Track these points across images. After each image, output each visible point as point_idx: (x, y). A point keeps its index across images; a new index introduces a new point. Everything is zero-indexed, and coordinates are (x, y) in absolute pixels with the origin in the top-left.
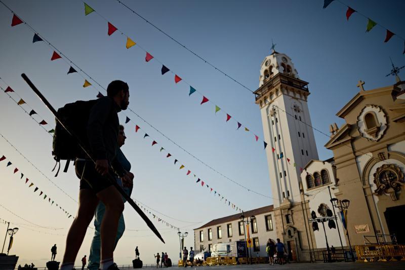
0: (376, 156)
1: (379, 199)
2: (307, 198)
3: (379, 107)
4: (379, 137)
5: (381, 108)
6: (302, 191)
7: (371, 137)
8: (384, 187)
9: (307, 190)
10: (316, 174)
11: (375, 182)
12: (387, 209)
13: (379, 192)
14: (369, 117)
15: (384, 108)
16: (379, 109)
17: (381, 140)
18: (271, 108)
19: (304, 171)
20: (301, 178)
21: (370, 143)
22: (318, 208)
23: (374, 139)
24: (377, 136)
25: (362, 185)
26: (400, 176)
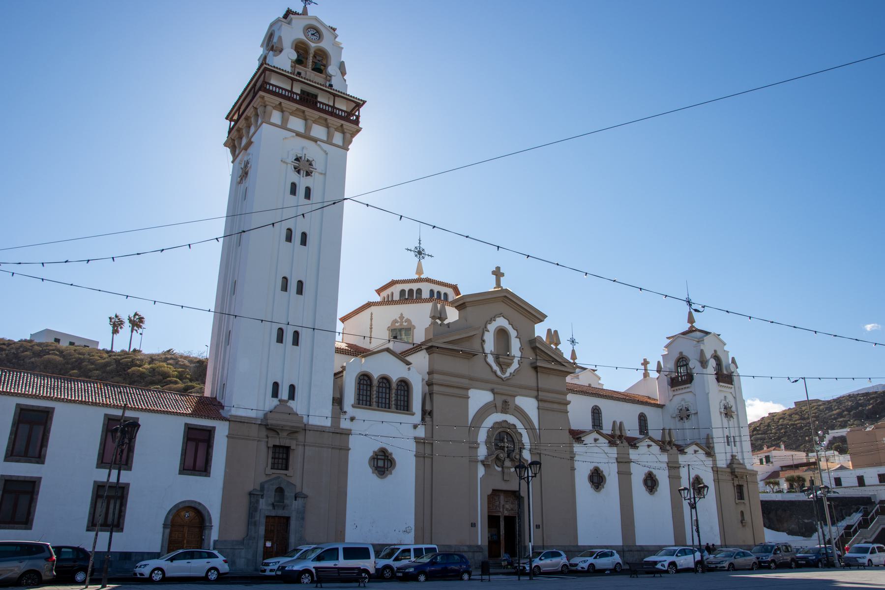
0: (499, 405)
2: (345, 424)
4: (507, 374)
6: (338, 401)
7: (496, 367)
9: (353, 406)
10: (385, 380)
12: (494, 490)
22: (371, 454)
24: (503, 371)
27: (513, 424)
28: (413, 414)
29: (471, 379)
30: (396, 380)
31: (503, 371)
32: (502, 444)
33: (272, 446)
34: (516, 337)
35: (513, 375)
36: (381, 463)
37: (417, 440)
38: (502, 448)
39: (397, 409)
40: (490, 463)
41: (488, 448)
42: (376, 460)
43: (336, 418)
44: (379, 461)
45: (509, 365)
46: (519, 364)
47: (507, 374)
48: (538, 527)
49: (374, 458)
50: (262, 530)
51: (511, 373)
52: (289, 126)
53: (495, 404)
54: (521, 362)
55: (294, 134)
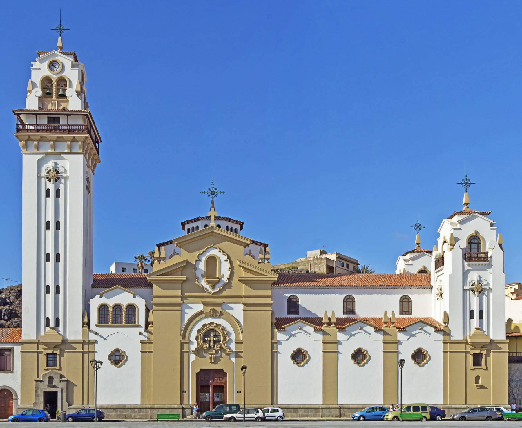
3: (227, 254)
5: (229, 257)
8: (207, 347)
9: (97, 326)
10: (117, 307)
11: (197, 338)
12: (201, 370)
13: (197, 352)
14: (212, 261)
15: (232, 260)
16: (226, 257)
18: (50, 165)
19: (98, 297)
20: (89, 305)
23: (210, 290)
25: (180, 338)
26: (225, 339)
30: (126, 306)
33: (46, 354)
36: (118, 358)
37: (142, 342)
39: (126, 324)
42: (114, 356)
43: (86, 334)
49: (113, 355)
50: (42, 399)
52: (41, 151)
55: (44, 155)
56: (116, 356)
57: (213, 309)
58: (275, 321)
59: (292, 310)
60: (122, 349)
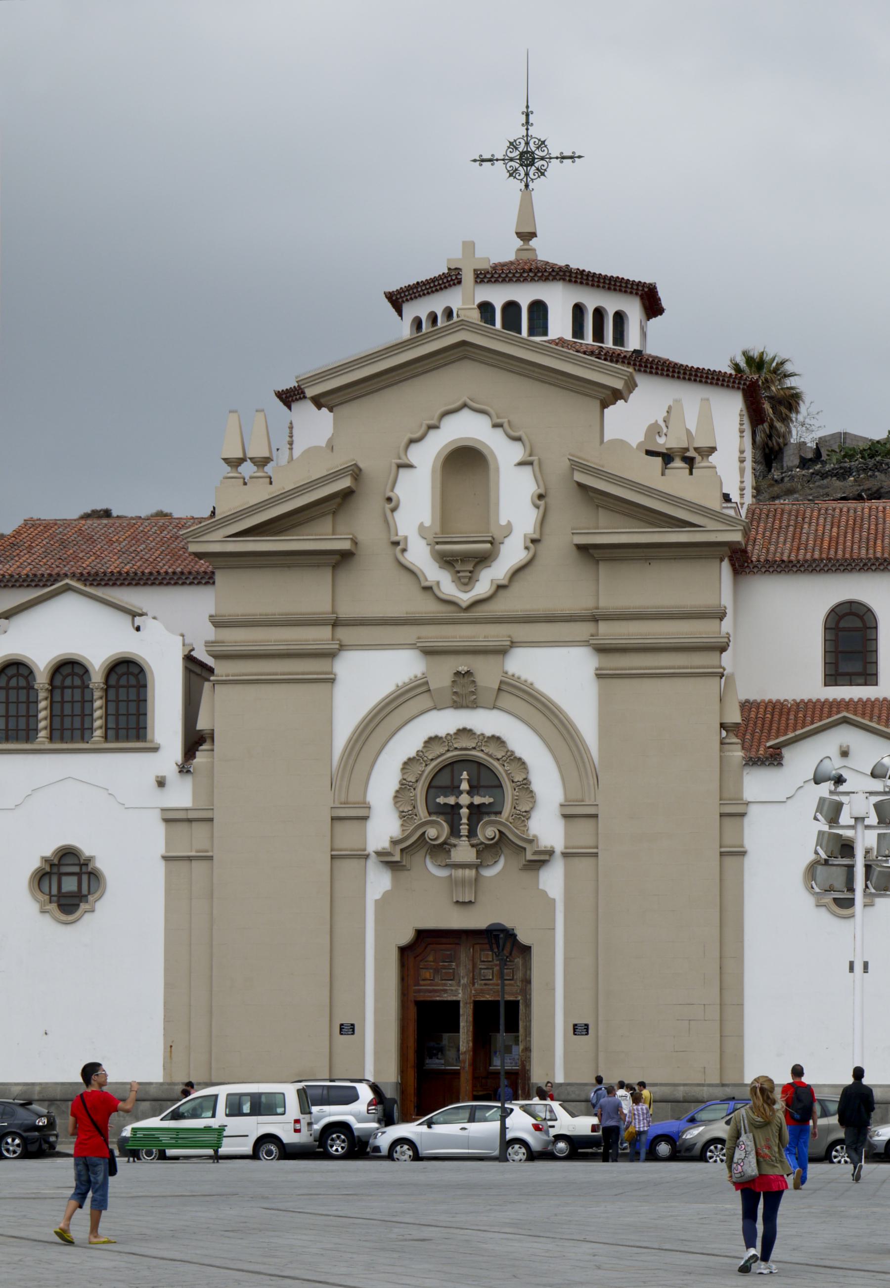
1: (395, 881)
4: (482, 587)
17: (477, 613)
21: (427, 607)
22: (35, 864)
24: (467, 581)
27: (493, 736)
28: (155, 749)
29: (336, 623)
31: (467, 581)
32: (451, 800)
34: (521, 464)
35: (500, 587)
36: (70, 885)
38: (451, 813)
40: (397, 858)
41: (405, 817)
44: (65, 879)
45: (483, 559)
46: (527, 548)
47: (482, 587)
48: (581, 1029)
51: (492, 581)
53: (427, 683)
54: (534, 541)
56: (74, 879)
57: (468, 673)
58: (734, 716)
59: (844, 668)
60: (87, 850)
